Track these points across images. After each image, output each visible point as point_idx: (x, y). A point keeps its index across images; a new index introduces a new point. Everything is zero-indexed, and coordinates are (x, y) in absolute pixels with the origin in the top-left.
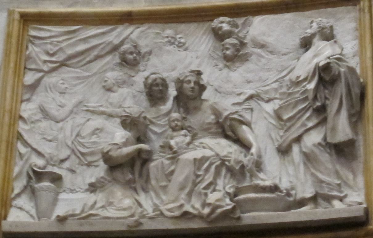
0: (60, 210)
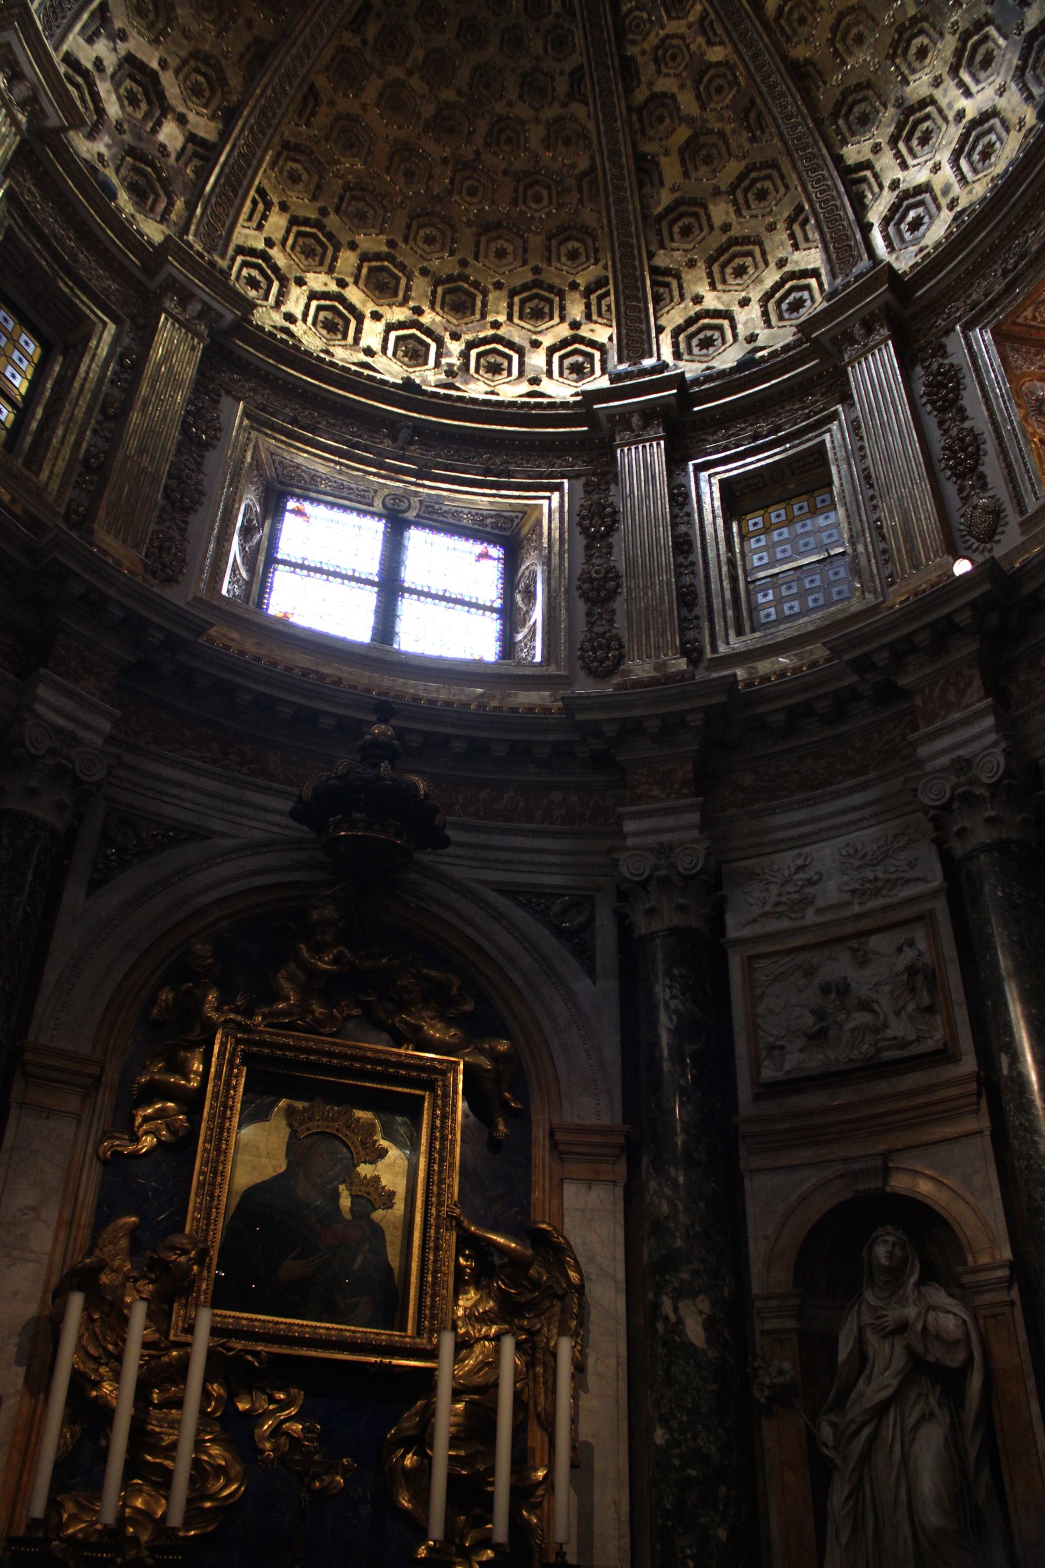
0: (787, 1066)
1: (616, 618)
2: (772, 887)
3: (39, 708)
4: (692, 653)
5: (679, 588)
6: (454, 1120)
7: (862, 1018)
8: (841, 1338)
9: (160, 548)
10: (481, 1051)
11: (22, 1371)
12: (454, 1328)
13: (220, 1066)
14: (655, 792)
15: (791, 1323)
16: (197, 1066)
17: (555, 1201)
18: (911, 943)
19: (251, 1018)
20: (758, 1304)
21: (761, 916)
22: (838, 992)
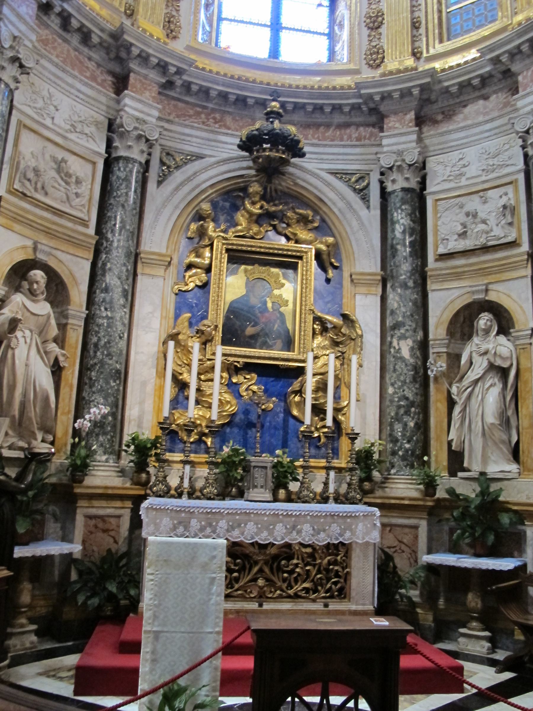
0: (449, 248)
1: (382, 37)
2: (447, 168)
3: (126, 109)
4: (416, 54)
5: (412, 19)
6: (311, 272)
7: (482, 227)
8: (463, 356)
9: (169, 22)
10: (321, 243)
11: (155, 370)
12: (313, 351)
13: (217, 254)
14: (397, 125)
15: (445, 350)
16: (207, 254)
17: (353, 302)
18: (506, 194)
19: (227, 234)
20: (431, 343)
21: (442, 181)
22: (473, 216)
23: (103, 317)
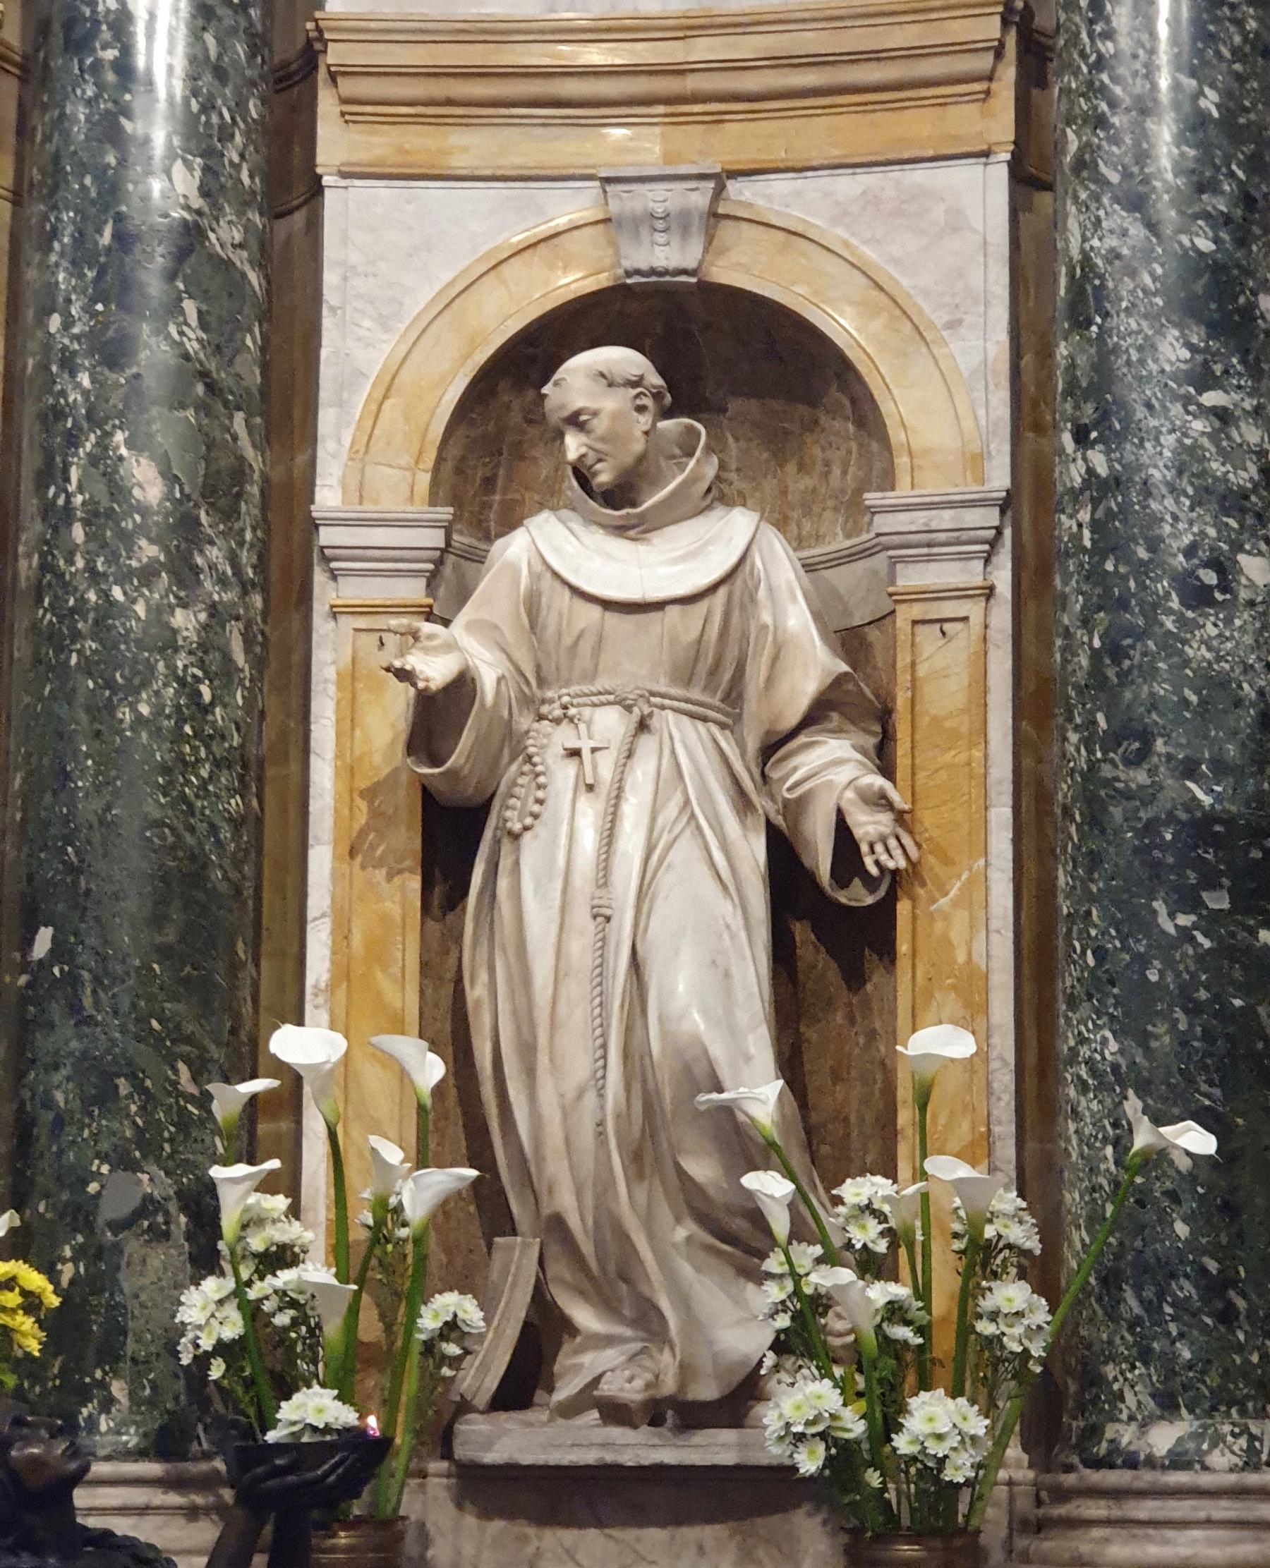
23: (1075, 494)
